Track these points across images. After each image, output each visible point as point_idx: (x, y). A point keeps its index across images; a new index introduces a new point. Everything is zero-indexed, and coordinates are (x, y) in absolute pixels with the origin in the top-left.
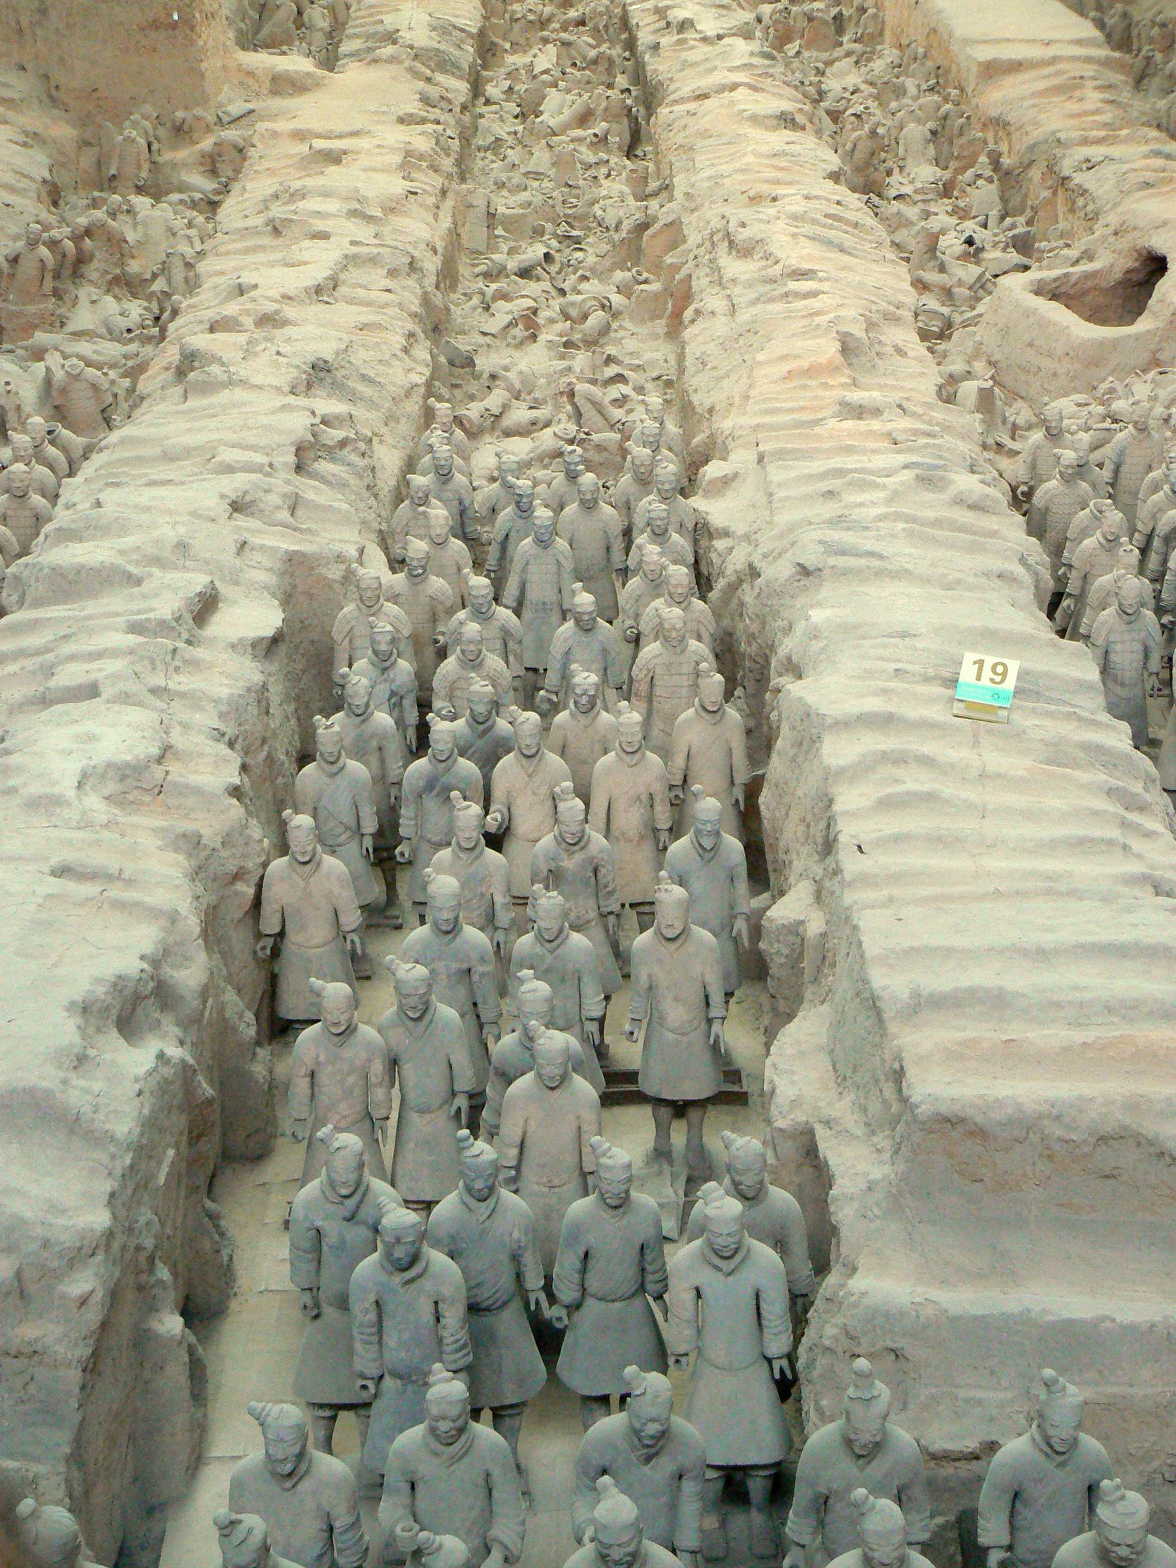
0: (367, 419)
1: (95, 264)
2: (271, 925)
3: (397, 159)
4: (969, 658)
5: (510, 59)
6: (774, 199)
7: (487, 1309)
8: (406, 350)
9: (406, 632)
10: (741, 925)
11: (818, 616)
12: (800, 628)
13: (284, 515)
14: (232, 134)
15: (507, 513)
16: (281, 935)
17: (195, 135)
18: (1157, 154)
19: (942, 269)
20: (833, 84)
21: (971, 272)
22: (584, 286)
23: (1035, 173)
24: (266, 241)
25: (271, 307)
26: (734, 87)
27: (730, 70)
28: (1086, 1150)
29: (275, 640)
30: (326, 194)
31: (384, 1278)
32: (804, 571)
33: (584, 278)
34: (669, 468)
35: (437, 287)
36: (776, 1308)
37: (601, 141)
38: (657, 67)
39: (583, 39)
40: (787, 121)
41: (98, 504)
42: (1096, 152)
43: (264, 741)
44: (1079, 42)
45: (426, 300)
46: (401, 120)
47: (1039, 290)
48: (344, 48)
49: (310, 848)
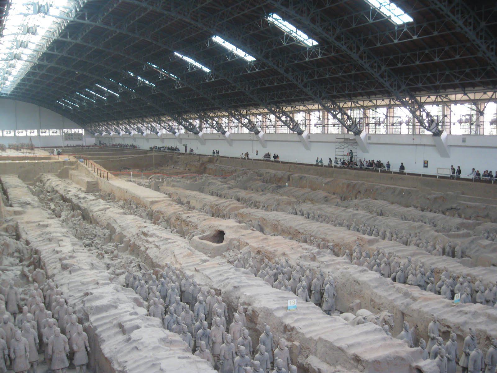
6: (145, 227)
12: (243, 296)
14: (11, 223)
22: (103, 247)
23: (173, 220)
24: (48, 243)
25: (70, 254)
26: (108, 208)
27: (103, 205)
30: (56, 232)
32: (235, 287)
33: (102, 245)
38: (83, 205)
40: (125, 214)
41: (91, 294)
42: (189, 215)
44: (164, 197)
46: (48, 218)
47: (200, 238)
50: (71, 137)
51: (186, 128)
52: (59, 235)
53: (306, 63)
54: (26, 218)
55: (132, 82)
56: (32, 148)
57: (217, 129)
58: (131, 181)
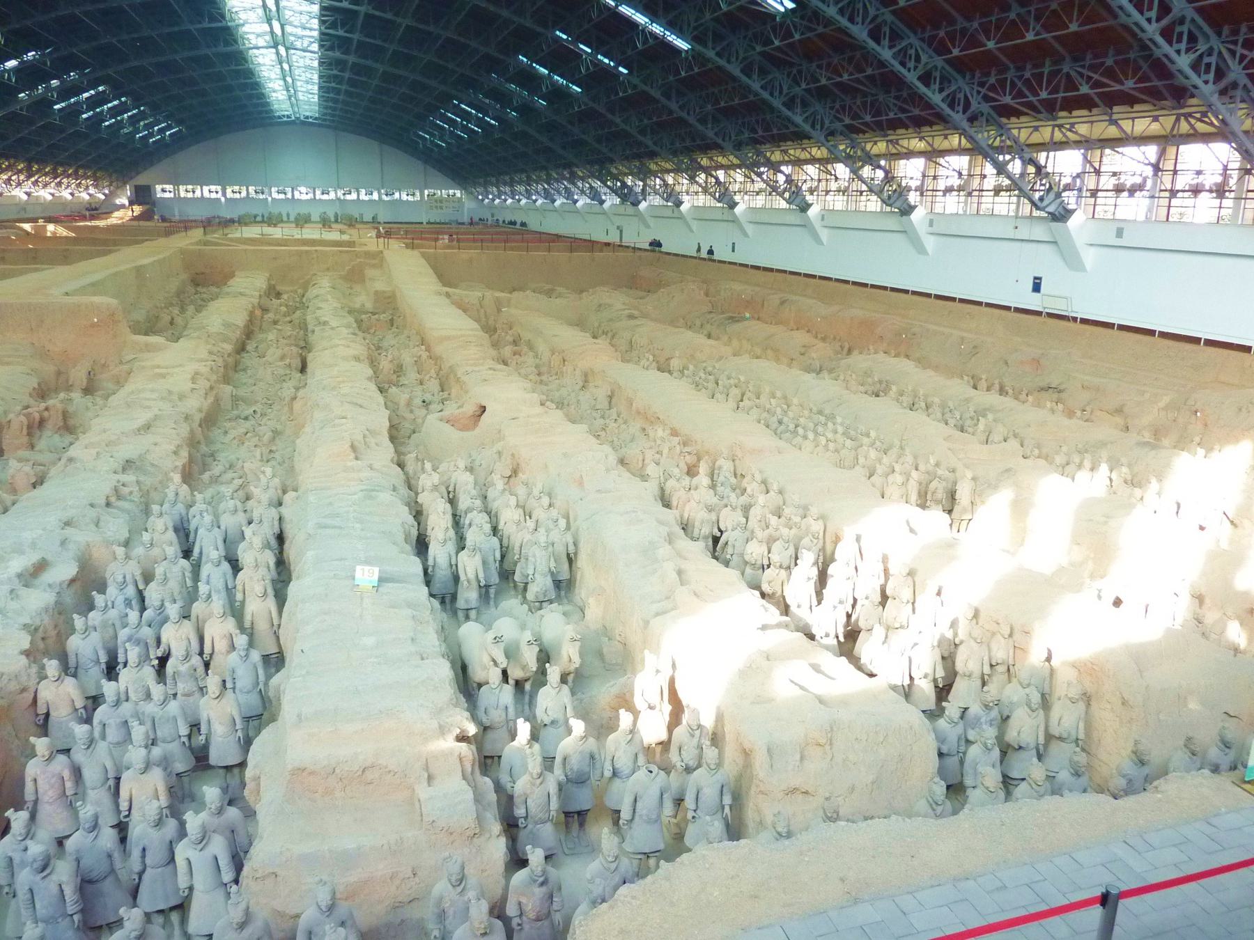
0: (148, 481)
1: (50, 422)
2: (42, 710)
3: (189, 376)
4: (359, 568)
5: (261, 336)
7: (97, 881)
8: (175, 453)
9: (138, 573)
10: (261, 686)
11: (310, 554)
13: (93, 527)
15: (198, 517)
16: (47, 715)
17: (111, 368)
18: (490, 369)
19: (411, 411)
20: (385, 344)
21: (424, 411)
22: (268, 423)
23: (452, 376)
25: (113, 438)
28: (358, 773)
29: (72, 581)
30: (152, 391)
31: (32, 877)
34: (265, 498)
35: (200, 425)
36: (224, 862)
37: (289, 365)
38: (312, 338)
39: (288, 330)
40: (357, 359)
42: (469, 369)
43: (56, 626)
44: (472, 330)
45: (192, 432)
48: (185, 333)
49: (57, 674)
50: (439, 204)
51: (614, 191)
52: (154, 396)
53: (778, 48)
54: (160, 359)
55: (502, 98)
56: (352, 222)
57: (717, 194)
58: (448, 295)
